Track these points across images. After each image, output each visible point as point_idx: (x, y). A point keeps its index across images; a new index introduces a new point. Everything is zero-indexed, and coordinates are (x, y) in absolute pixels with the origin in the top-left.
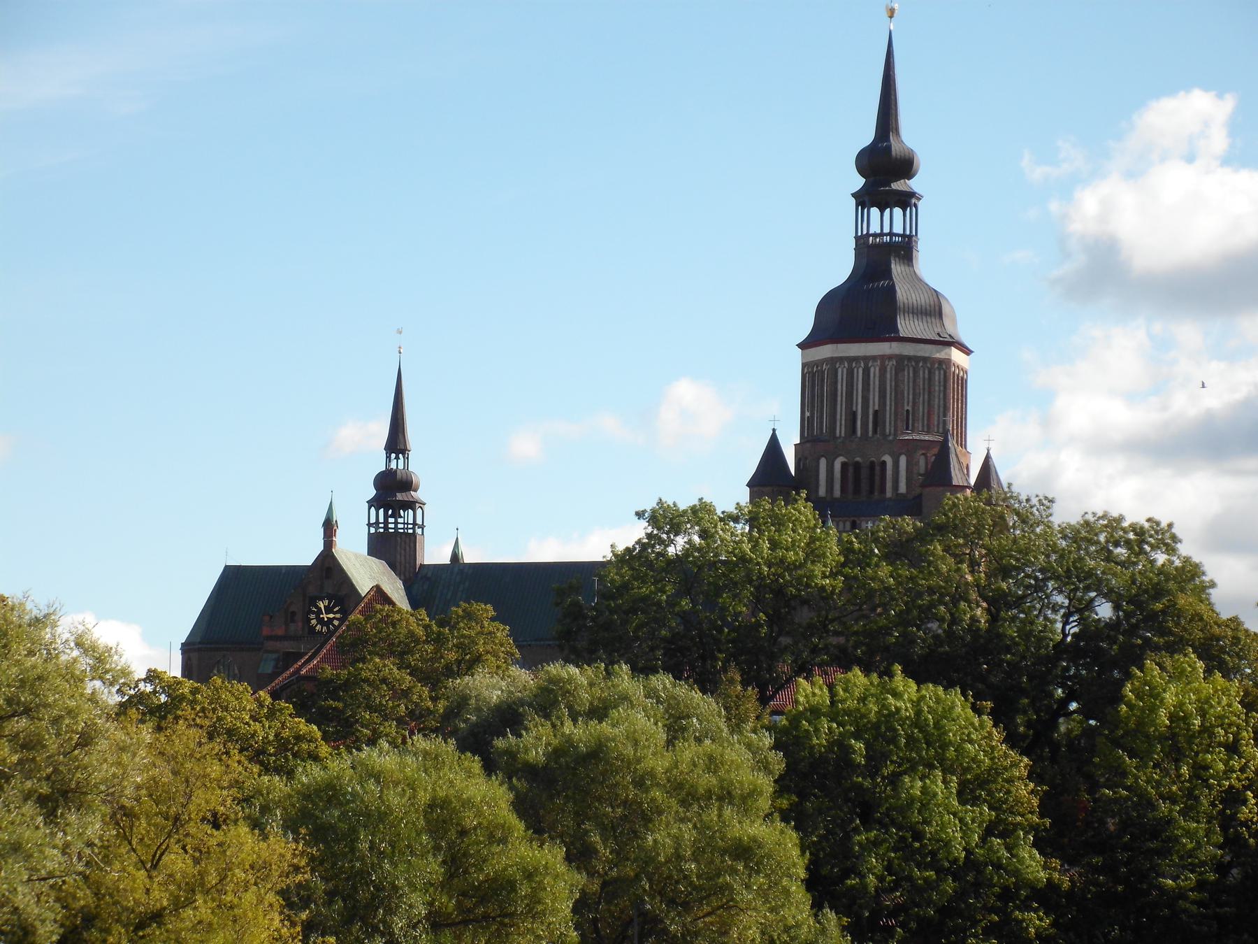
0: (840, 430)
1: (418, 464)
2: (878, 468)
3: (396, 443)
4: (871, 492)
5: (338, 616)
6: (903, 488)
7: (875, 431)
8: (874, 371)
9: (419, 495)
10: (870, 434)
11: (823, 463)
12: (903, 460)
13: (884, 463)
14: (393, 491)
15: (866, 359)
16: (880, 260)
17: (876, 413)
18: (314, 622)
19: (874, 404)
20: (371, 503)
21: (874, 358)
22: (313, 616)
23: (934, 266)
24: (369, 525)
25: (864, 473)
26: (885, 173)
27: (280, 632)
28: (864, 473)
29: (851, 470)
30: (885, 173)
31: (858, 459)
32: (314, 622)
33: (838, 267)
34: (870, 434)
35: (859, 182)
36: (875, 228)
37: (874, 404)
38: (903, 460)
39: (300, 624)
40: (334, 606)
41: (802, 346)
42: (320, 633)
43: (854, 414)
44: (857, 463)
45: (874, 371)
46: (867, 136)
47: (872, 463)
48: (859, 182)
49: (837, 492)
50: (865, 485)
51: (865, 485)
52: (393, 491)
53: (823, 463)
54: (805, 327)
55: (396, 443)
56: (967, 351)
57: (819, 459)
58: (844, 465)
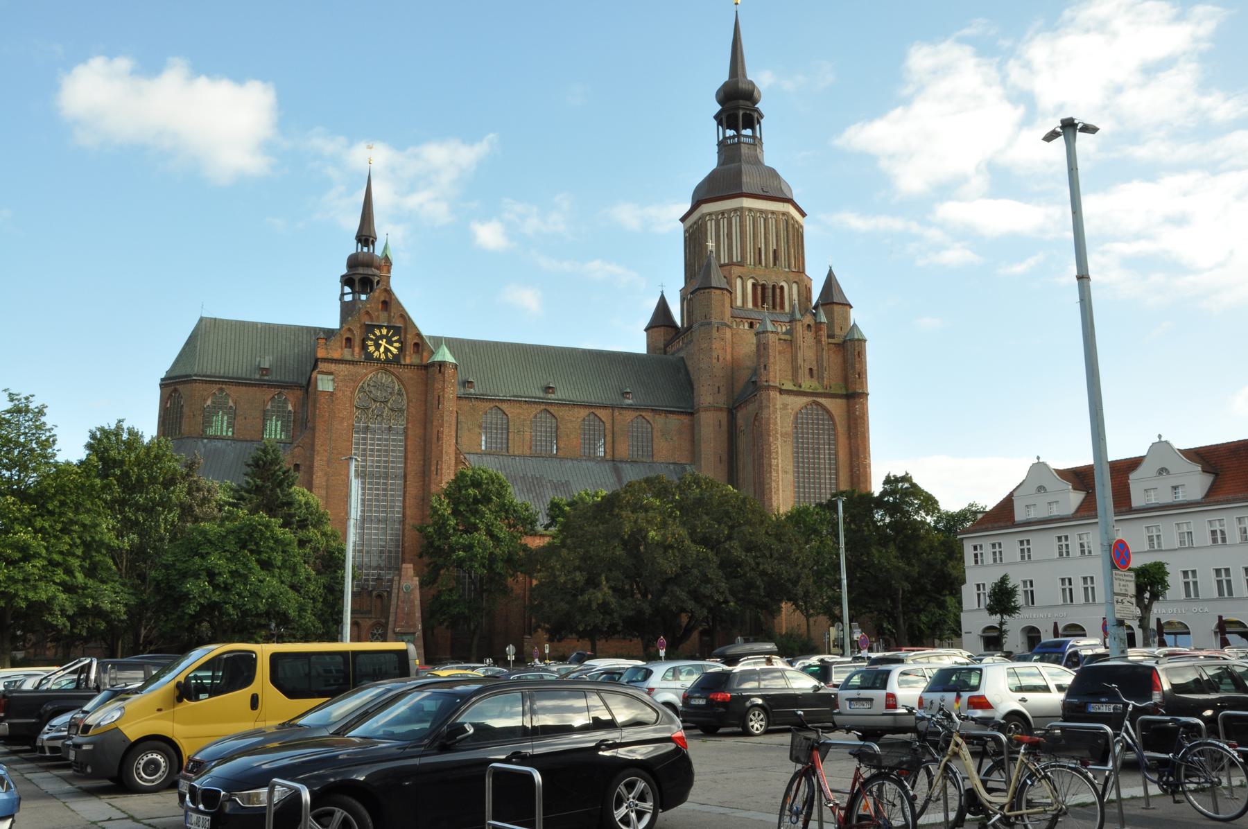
0: (750, 259)
2: (778, 291)
3: (365, 236)
5: (397, 345)
7: (775, 264)
8: (772, 222)
11: (739, 282)
13: (782, 288)
17: (775, 251)
18: (372, 349)
20: (347, 281)
21: (773, 213)
22: (370, 343)
27: (336, 355)
29: (759, 289)
32: (372, 349)
35: (719, 107)
38: (795, 287)
39: (357, 350)
40: (393, 335)
42: (378, 360)
46: (724, 77)
49: (750, 305)
58: (754, 285)
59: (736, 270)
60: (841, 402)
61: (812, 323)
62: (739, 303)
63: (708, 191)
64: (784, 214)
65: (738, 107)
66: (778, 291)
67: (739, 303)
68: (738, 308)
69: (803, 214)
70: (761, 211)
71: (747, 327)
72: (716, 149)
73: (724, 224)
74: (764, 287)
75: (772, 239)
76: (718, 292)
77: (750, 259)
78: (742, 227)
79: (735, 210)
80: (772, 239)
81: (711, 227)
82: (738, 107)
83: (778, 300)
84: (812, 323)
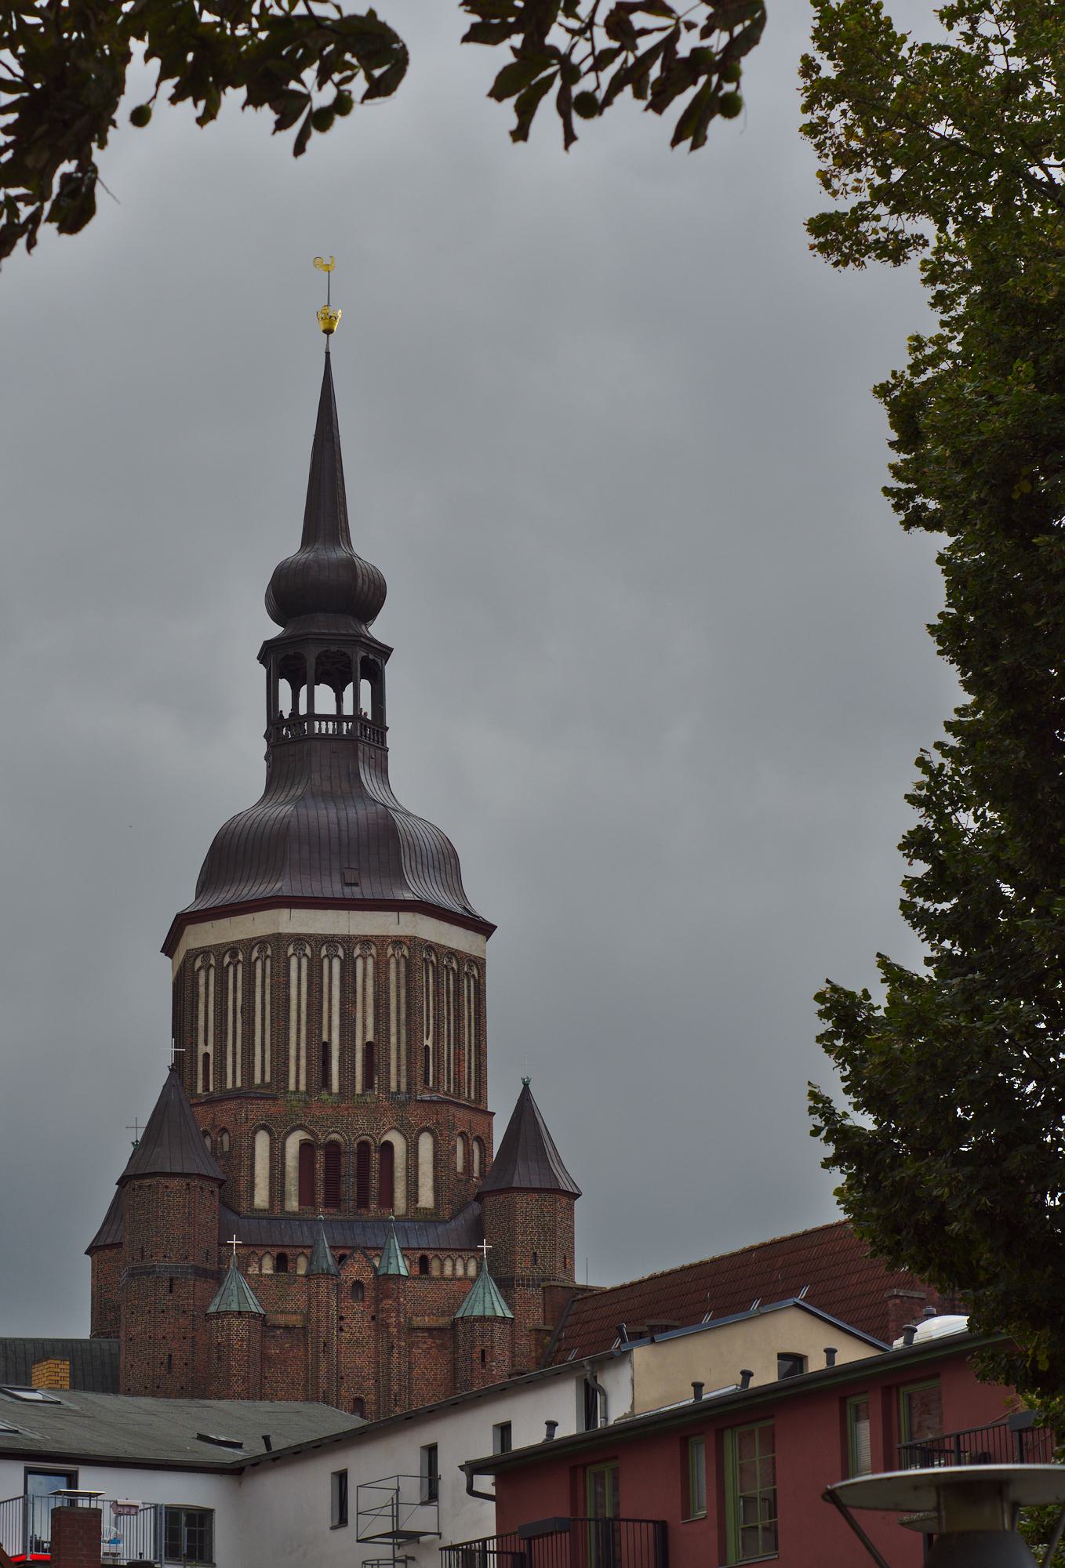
0: (297, 1078)
2: (375, 1157)
4: (363, 1202)
6: (426, 1198)
7: (368, 1084)
8: (364, 969)
10: (359, 1088)
11: (262, 1142)
12: (426, 1144)
13: (388, 1147)
15: (348, 941)
17: (369, 1047)
19: (365, 1031)
21: (366, 941)
25: (349, 1164)
28: (349, 1164)
29: (320, 1156)
31: (335, 1136)
33: (235, 776)
34: (359, 1088)
37: (365, 1031)
38: (426, 1144)
43: (326, 1047)
44: (334, 1144)
45: (364, 969)
46: (284, 540)
47: (364, 1147)
49: (293, 1204)
50: (349, 1188)
51: (349, 1188)
53: (262, 1142)
57: (255, 1132)
58: (304, 1146)
59: (256, 1110)
61: (367, 1277)
62: (261, 1198)
63: (238, 860)
64: (398, 942)
65: (324, 619)
66: (375, 1157)
67: (261, 1198)
68: (258, 1215)
69: (486, 929)
70: (331, 941)
71: (268, 1270)
72: (263, 746)
73: (236, 978)
76: (175, 1183)
77: (297, 1078)
78: (281, 986)
79: (262, 942)
81: (206, 984)
82: (324, 619)
83: (374, 1183)
84: (367, 1277)
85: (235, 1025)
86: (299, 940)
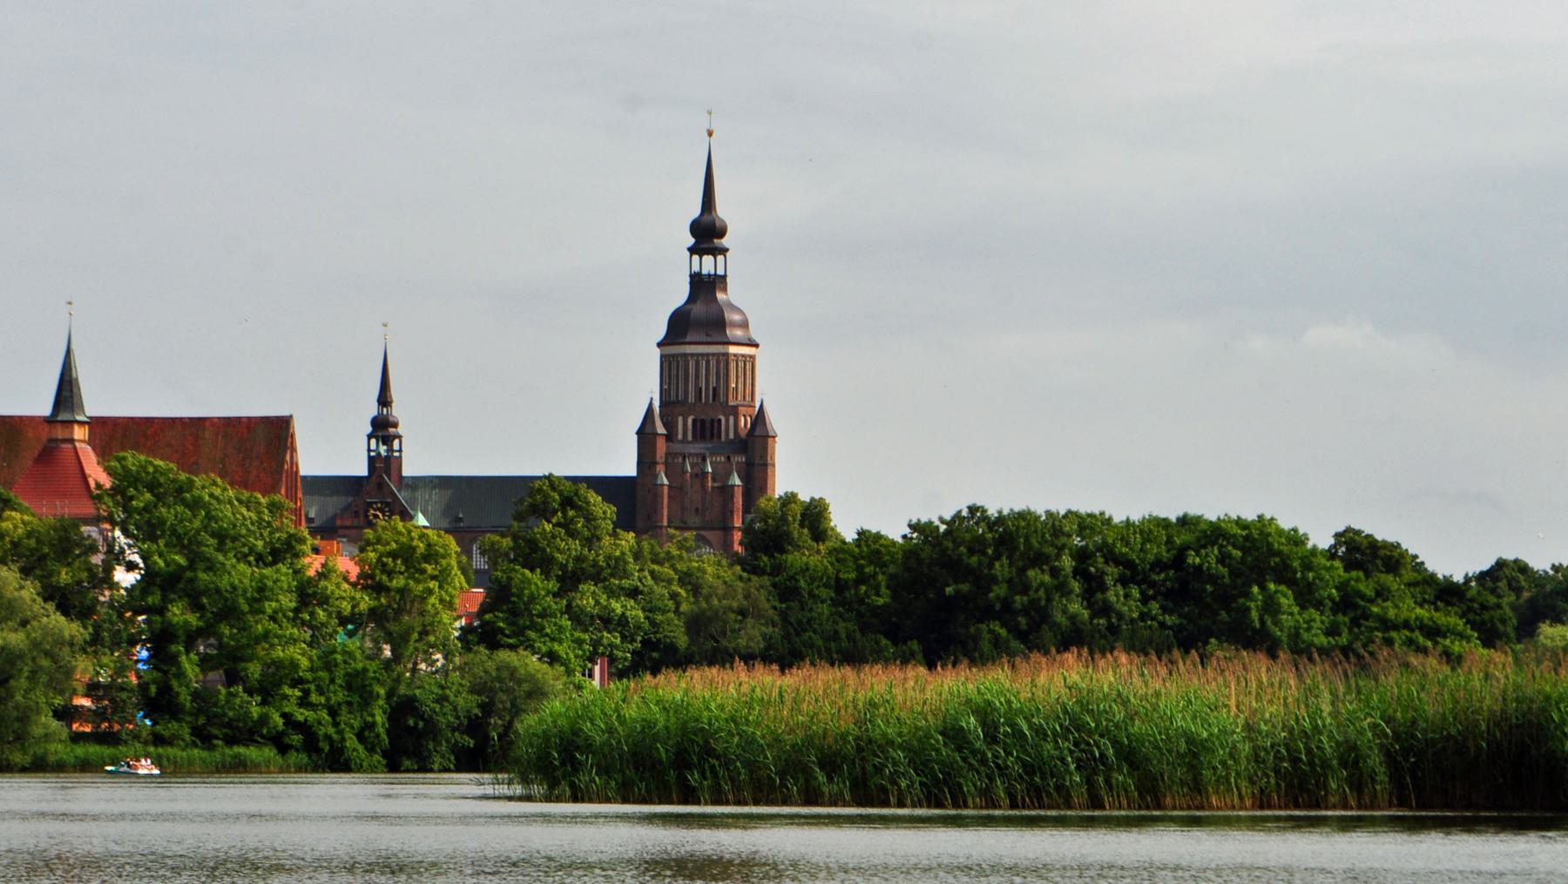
0: (691, 399)
1: (397, 411)
3: (384, 399)
6: (731, 436)
8: (713, 363)
9: (400, 430)
14: (382, 428)
15: (708, 355)
16: (704, 287)
20: (370, 437)
23: (735, 295)
24: (369, 450)
25: (708, 425)
26: (707, 235)
28: (708, 425)
30: (707, 235)
33: (679, 294)
35: (692, 241)
36: (696, 268)
41: (659, 345)
45: (713, 363)
46: (695, 211)
48: (692, 241)
49: (690, 438)
50: (708, 433)
52: (382, 428)
54: (661, 331)
55: (384, 399)
56: (757, 346)
60: (720, 533)
62: (680, 437)
67: (680, 437)
70: (702, 355)
73: (674, 365)
74: (703, 421)
75: (713, 380)
77: (691, 399)
80: (713, 380)
85: (674, 381)
86: (692, 355)
